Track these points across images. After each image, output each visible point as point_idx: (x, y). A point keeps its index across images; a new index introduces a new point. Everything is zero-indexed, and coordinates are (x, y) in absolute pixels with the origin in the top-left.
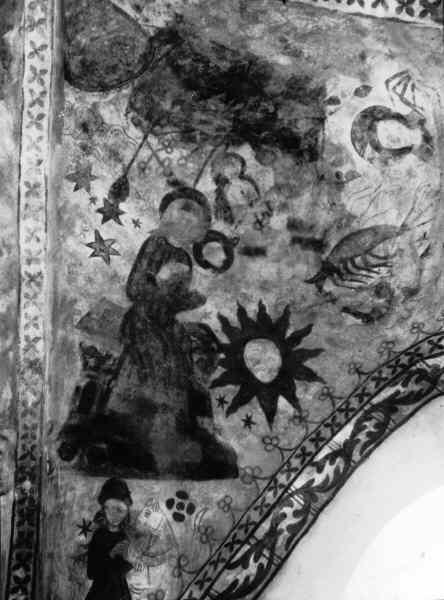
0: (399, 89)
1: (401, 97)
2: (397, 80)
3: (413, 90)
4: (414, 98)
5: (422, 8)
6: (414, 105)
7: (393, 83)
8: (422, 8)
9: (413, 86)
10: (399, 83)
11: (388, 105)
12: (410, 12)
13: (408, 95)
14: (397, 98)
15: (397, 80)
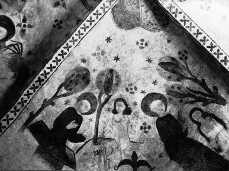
0: (16, 46)
1: (12, 45)
2: (20, 48)
3: (13, 51)
4: (10, 49)
5: (41, 79)
6: (8, 48)
7: (20, 45)
8: (41, 79)
9: (15, 52)
10: (19, 48)
11: (12, 39)
12: (42, 75)
13: (12, 48)
14: (14, 43)
15: (20, 48)
